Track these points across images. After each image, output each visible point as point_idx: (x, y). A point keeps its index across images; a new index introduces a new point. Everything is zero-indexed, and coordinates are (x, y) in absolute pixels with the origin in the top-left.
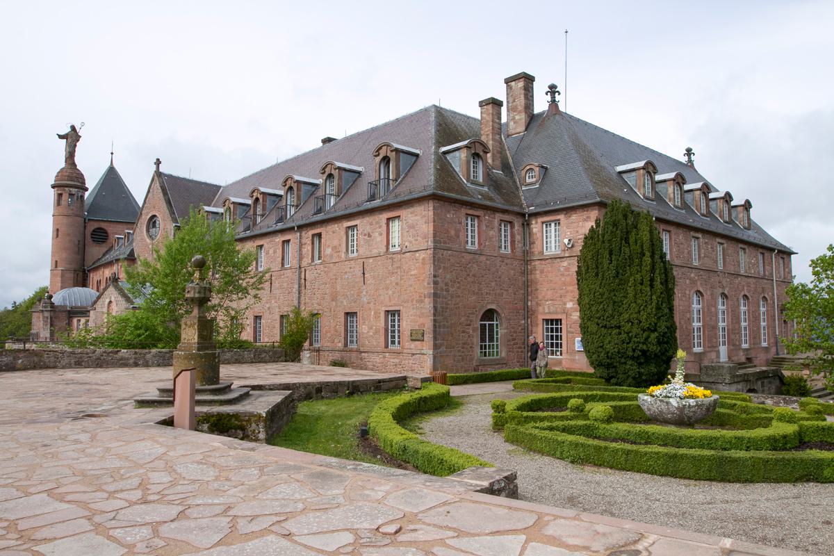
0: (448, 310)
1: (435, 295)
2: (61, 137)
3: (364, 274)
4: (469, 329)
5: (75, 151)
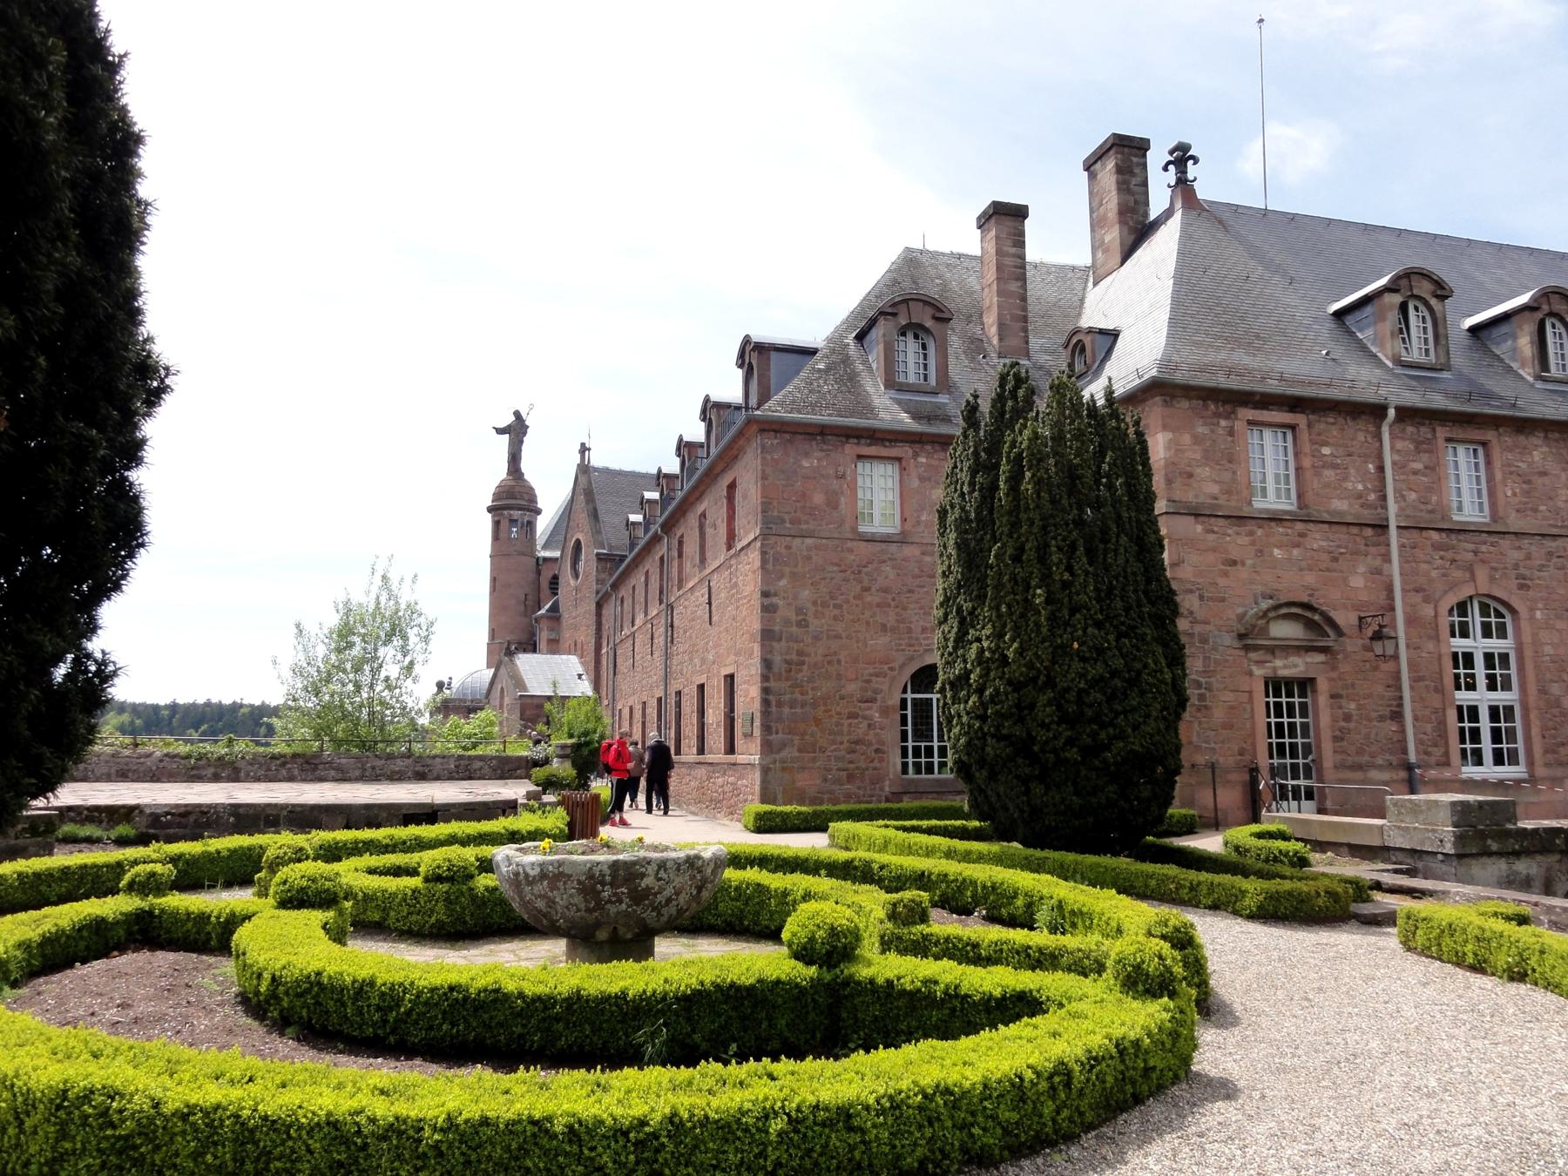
0: (805, 667)
1: (767, 635)
2: (500, 431)
3: (710, 603)
4: (870, 708)
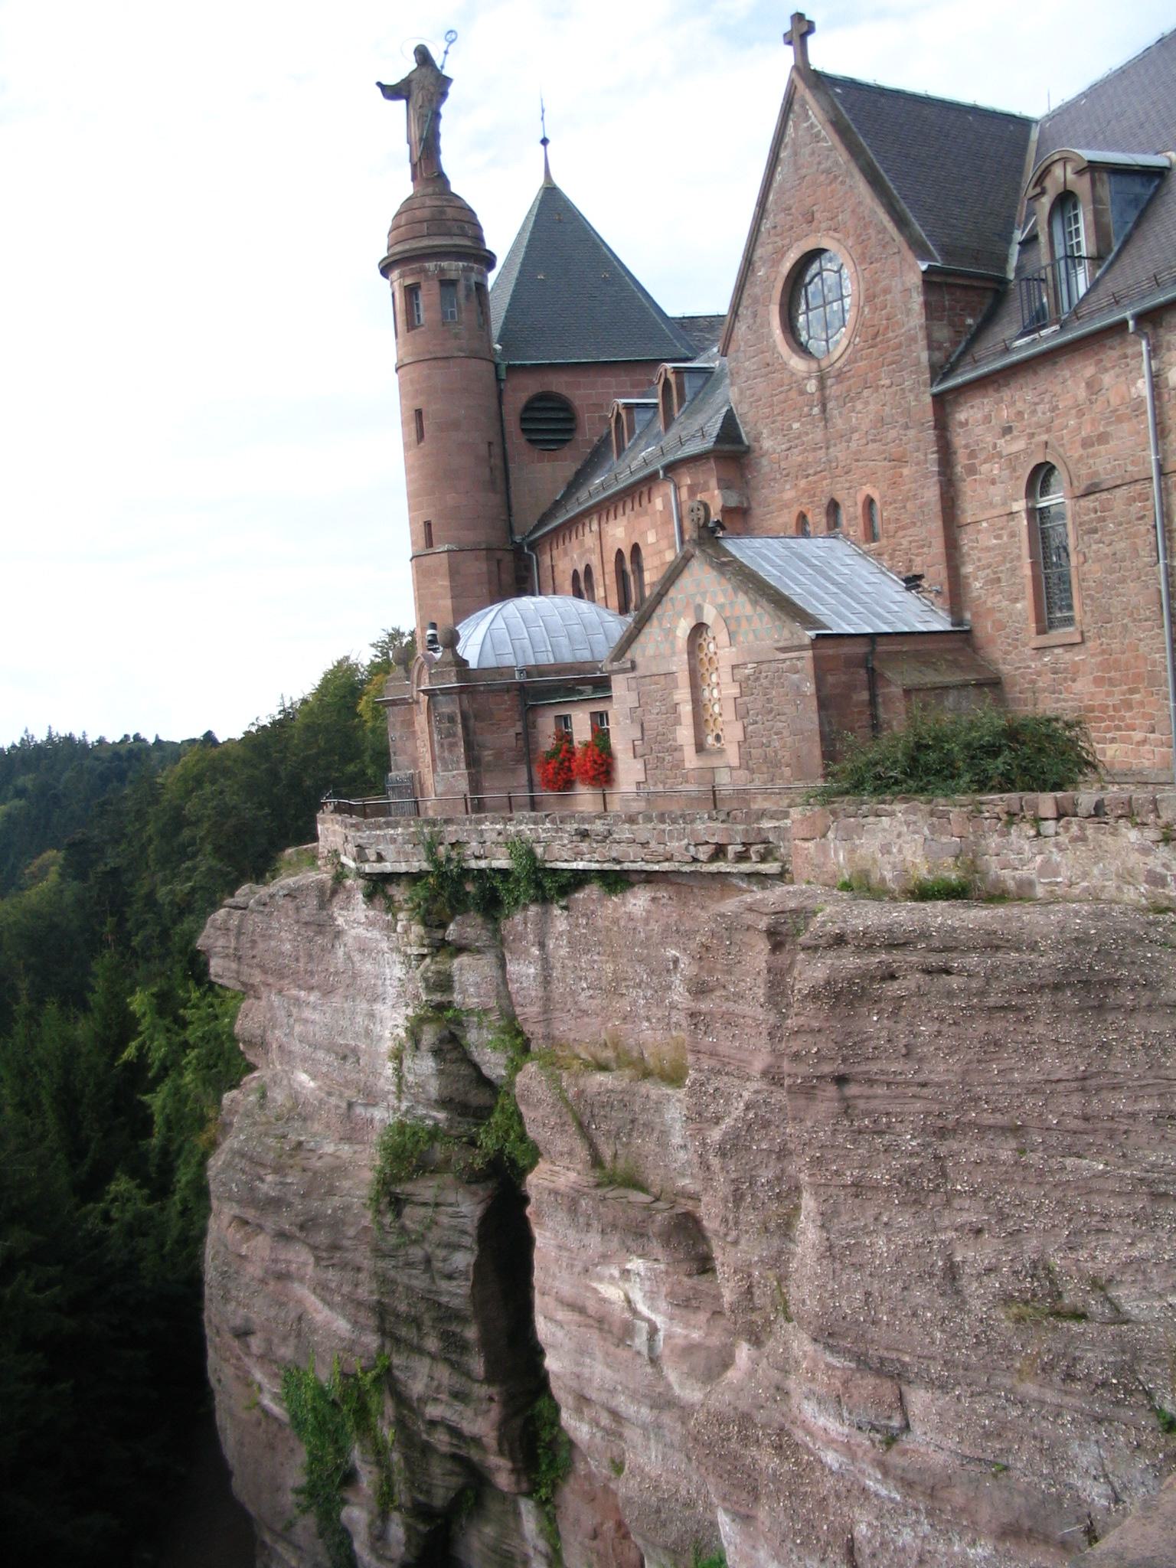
2: (391, 92)
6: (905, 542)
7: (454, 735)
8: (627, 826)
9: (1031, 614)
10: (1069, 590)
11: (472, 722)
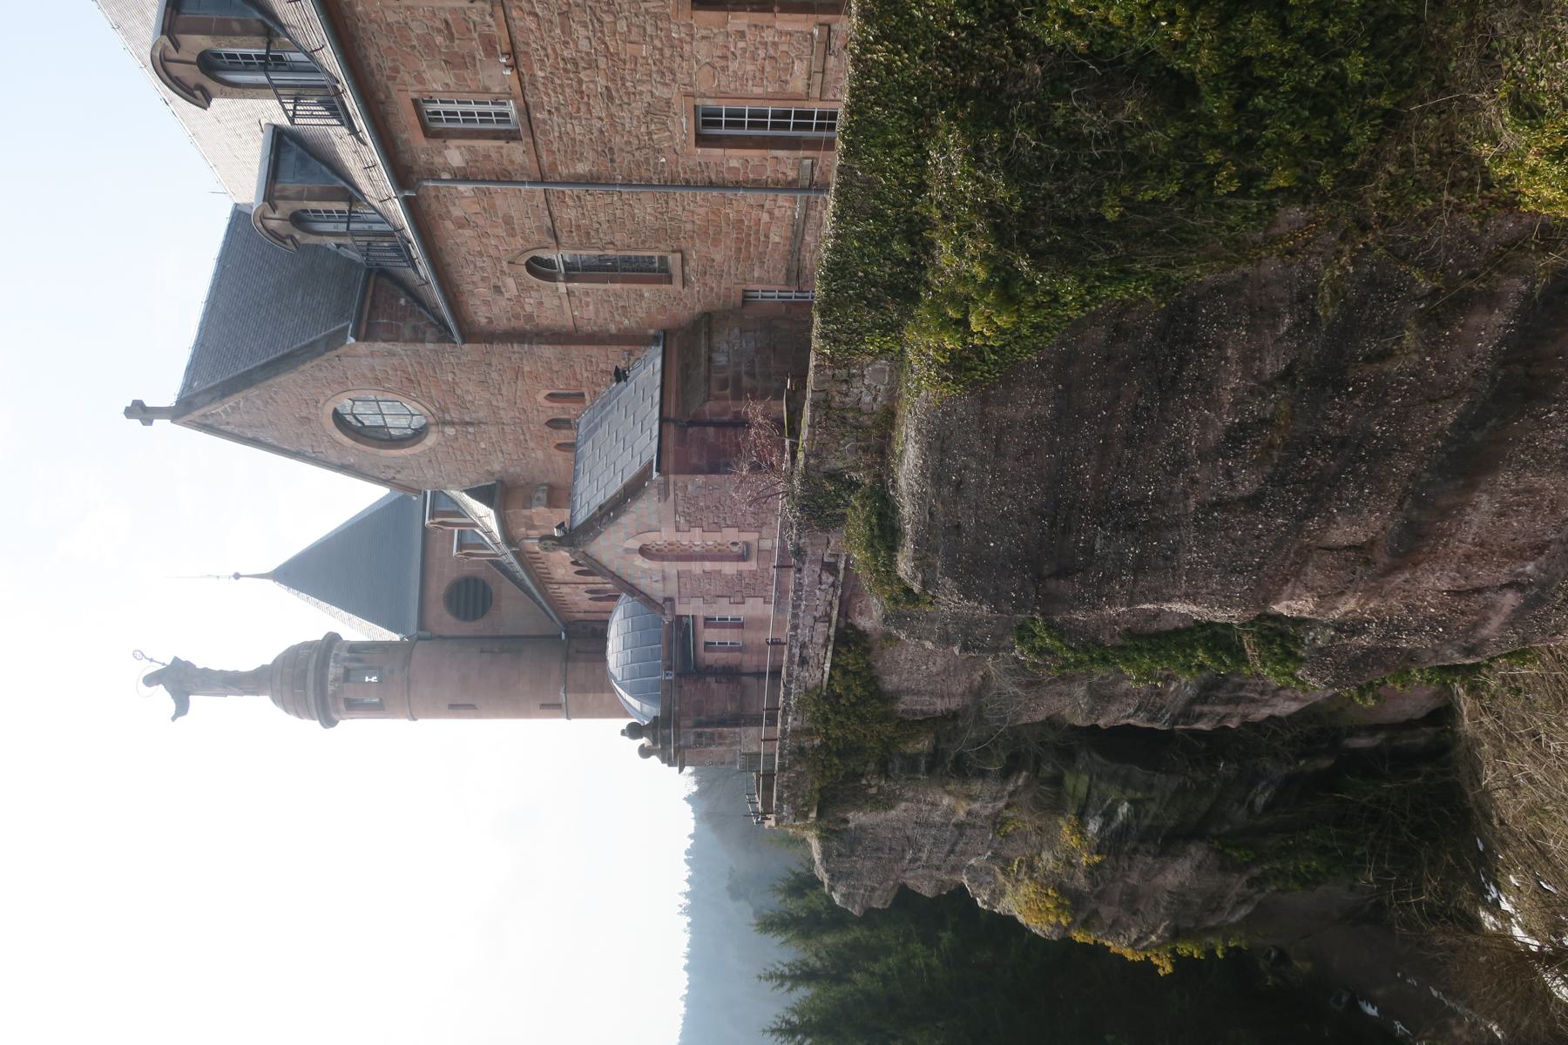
2: (182, 708)
5: (221, 671)
6: (585, 374)
7: (713, 734)
8: (799, 631)
9: (655, 287)
10: (636, 257)
11: (703, 718)
